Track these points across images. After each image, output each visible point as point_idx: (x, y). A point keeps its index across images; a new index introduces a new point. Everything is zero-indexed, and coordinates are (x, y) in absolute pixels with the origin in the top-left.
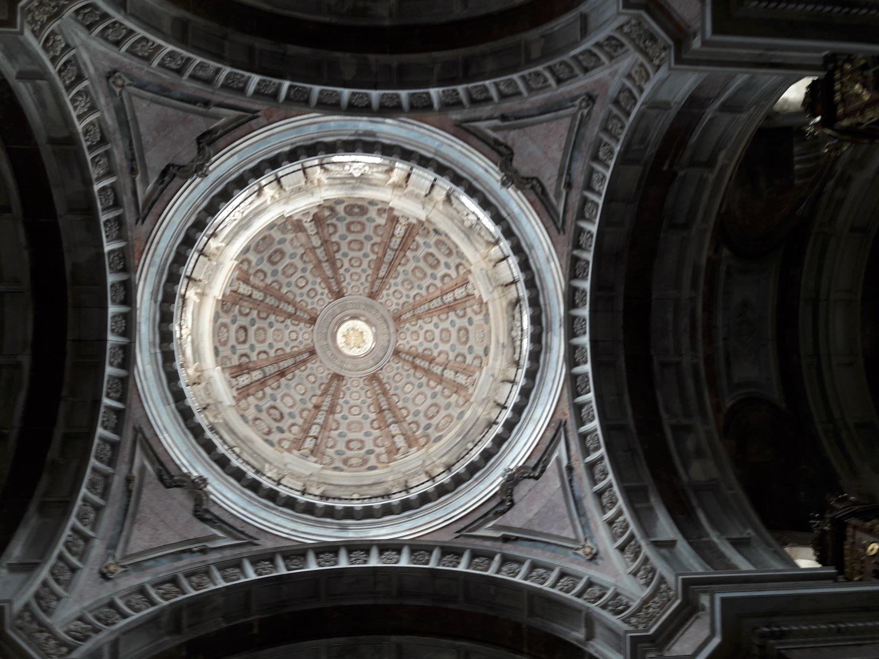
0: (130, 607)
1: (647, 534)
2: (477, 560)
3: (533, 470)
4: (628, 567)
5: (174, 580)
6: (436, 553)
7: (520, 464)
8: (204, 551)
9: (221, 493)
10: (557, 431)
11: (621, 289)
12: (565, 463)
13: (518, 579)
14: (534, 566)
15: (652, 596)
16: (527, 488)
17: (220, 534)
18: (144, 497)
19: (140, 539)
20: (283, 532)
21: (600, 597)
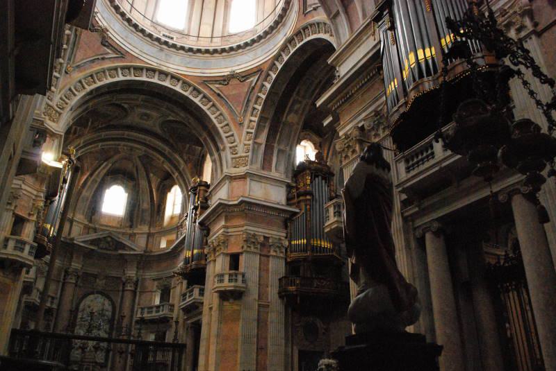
0: (76, 90)
1: (256, 137)
2: (204, 99)
3: (244, 76)
4: (245, 140)
5: (92, 76)
6: (191, 88)
7: (238, 71)
8: (103, 59)
9: (113, 30)
10: (258, 71)
11: (308, 54)
12: (253, 85)
13: (212, 117)
14: (221, 114)
15: (243, 157)
16: (235, 82)
17: (110, 52)
18: (82, 37)
19: (79, 55)
20: (135, 52)
21: (232, 143)
